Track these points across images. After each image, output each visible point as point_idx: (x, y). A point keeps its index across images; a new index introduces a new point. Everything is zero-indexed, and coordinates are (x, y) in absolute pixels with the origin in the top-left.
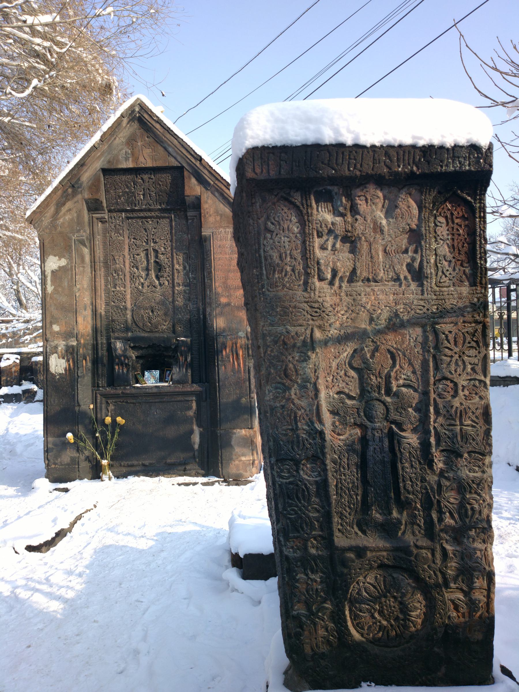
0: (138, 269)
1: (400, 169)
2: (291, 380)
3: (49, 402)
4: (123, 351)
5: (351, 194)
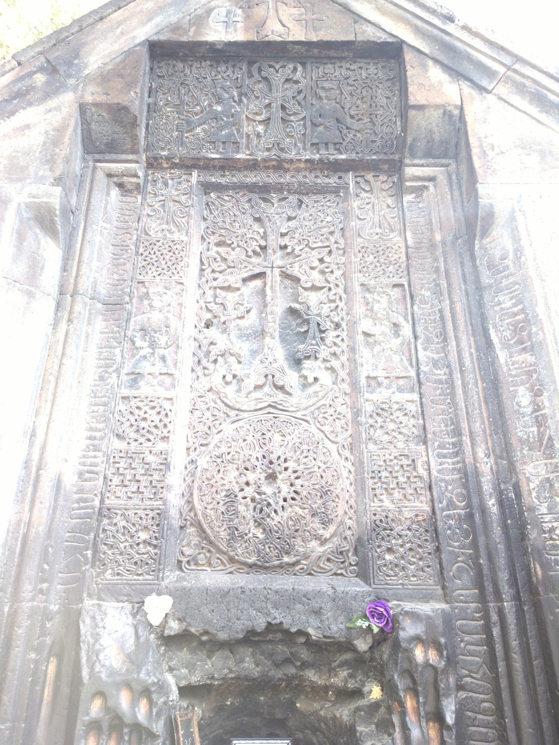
0: (224, 331)
4: (129, 658)
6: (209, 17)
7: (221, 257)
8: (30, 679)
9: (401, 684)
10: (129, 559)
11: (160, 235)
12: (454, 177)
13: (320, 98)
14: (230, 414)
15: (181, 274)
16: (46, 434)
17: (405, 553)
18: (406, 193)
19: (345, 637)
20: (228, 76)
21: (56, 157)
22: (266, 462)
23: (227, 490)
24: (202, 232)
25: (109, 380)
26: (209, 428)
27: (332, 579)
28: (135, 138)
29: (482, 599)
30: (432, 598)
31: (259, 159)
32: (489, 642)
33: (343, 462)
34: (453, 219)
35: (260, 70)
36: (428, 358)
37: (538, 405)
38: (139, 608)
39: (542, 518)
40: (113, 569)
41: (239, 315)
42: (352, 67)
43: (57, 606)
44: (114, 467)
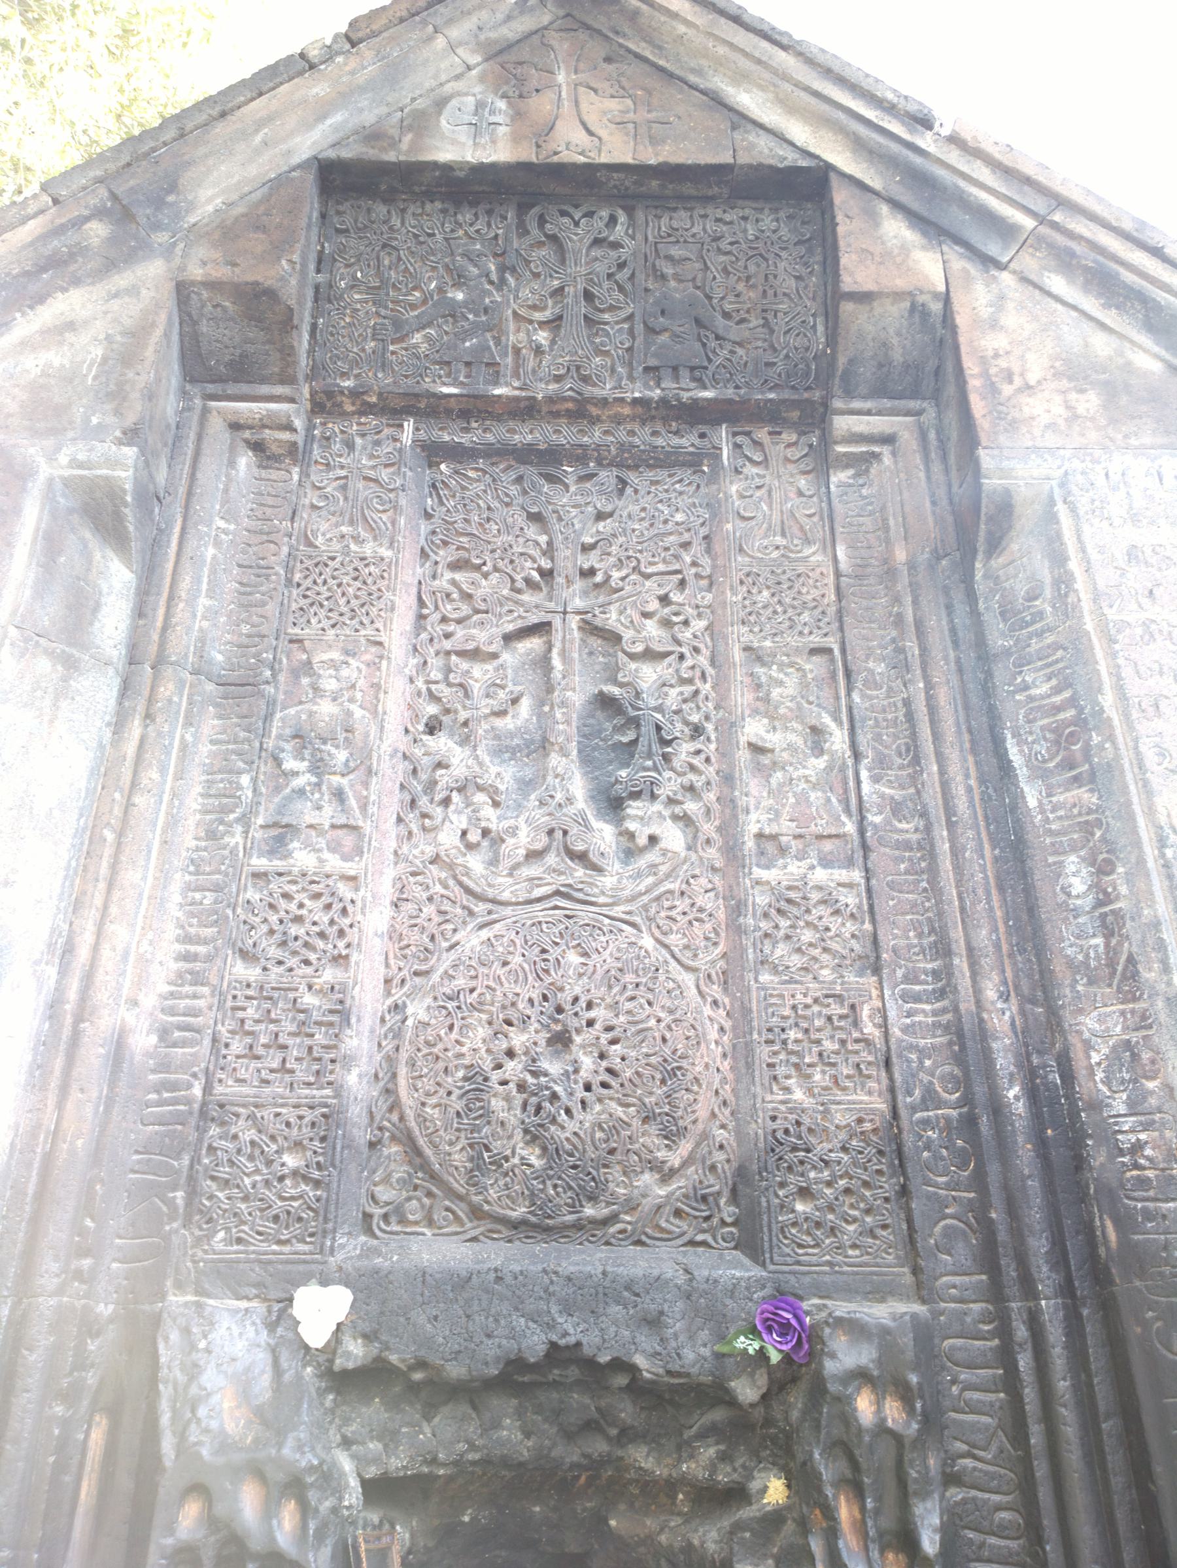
0: (465, 741)
6: (440, 113)
7: (461, 591)
8: (52, 1459)
9: (827, 1469)
10: (262, 1210)
11: (336, 546)
12: (932, 435)
13: (663, 277)
14: (476, 909)
15: (379, 625)
16: (96, 948)
17: (837, 1199)
18: (836, 468)
19: (713, 1374)
20: (477, 231)
21: (127, 387)
22: (549, 1007)
23: (467, 1067)
24: (422, 542)
25: (227, 839)
26: (432, 938)
27: (685, 1253)
28: (288, 353)
29: (996, 1293)
30: (892, 1293)
31: (540, 396)
32: (1011, 1383)
33: (708, 1011)
34: (930, 520)
35: (542, 221)
36: (882, 796)
37: (1105, 893)
38: (282, 1312)
39: (1116, 1123)
40: (228, 1230)
41: (496, 709)
42: (727, 217)
43: (111, 1307)
44: (233, 1018)
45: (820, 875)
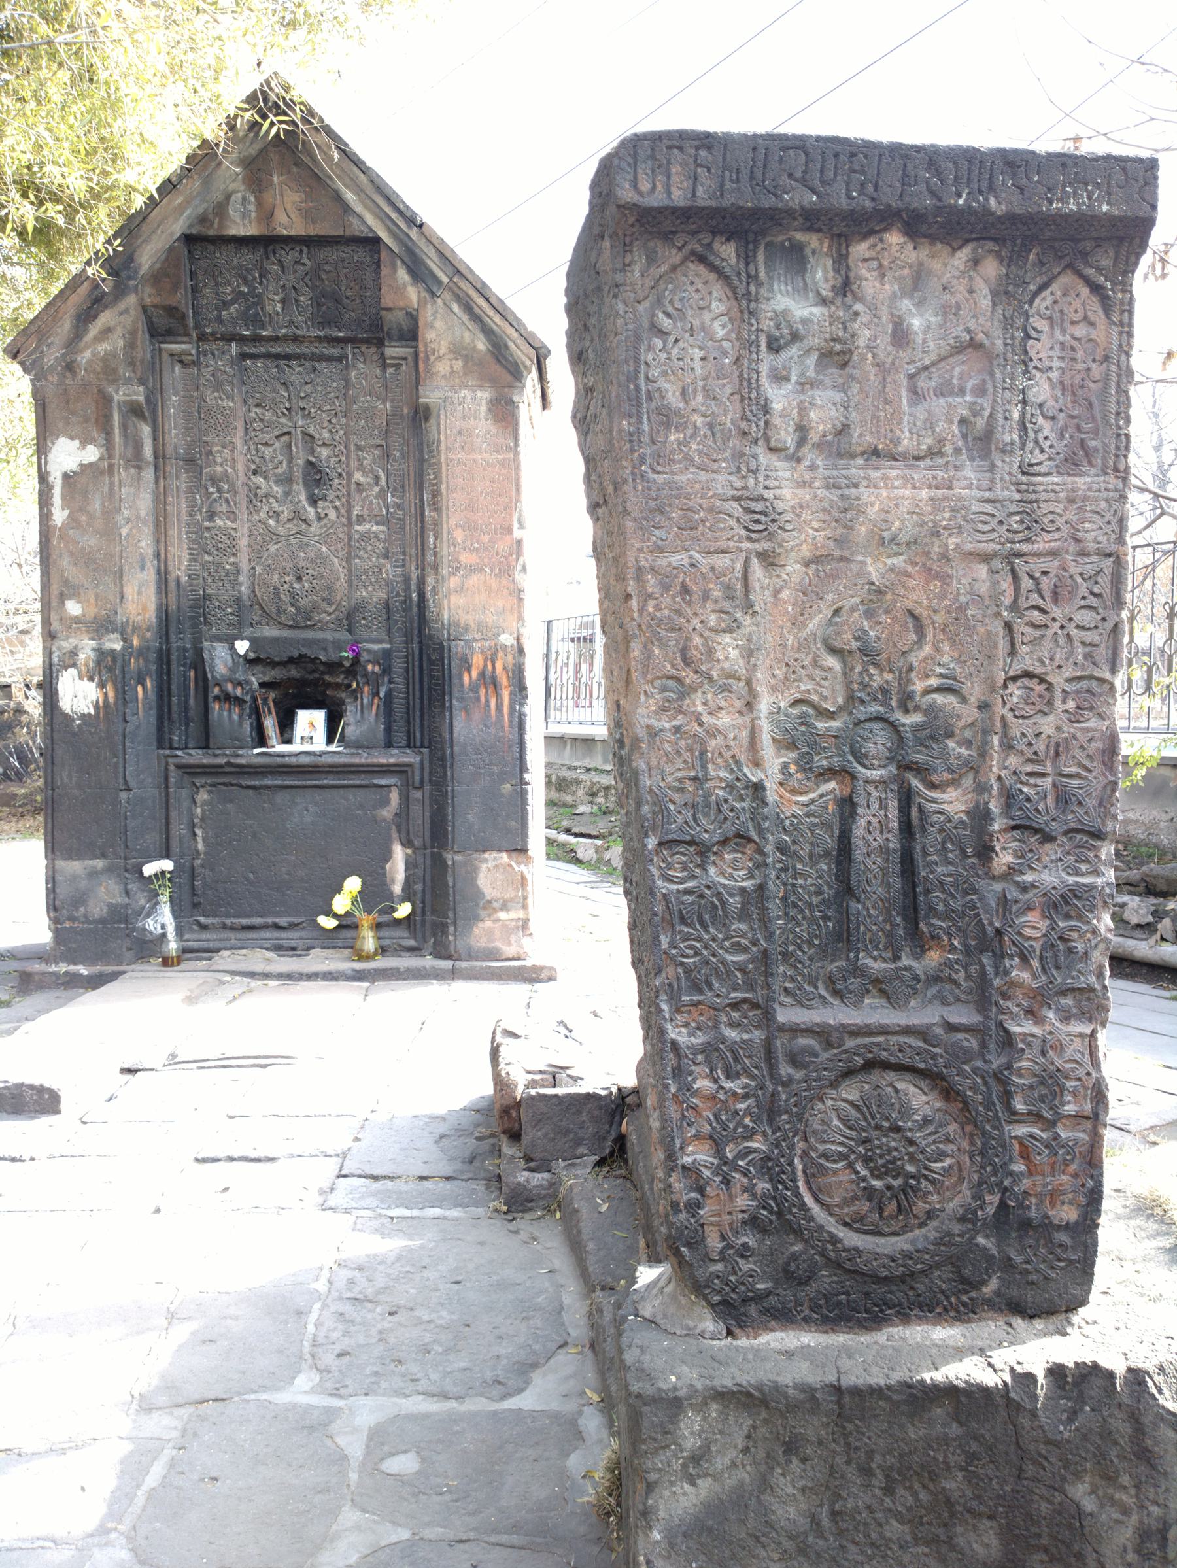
1: (961, 202)
2: (696, 672)
3: (57, 778)
5: (848, 253)
28: (186, 326)
45: (375, 528)
